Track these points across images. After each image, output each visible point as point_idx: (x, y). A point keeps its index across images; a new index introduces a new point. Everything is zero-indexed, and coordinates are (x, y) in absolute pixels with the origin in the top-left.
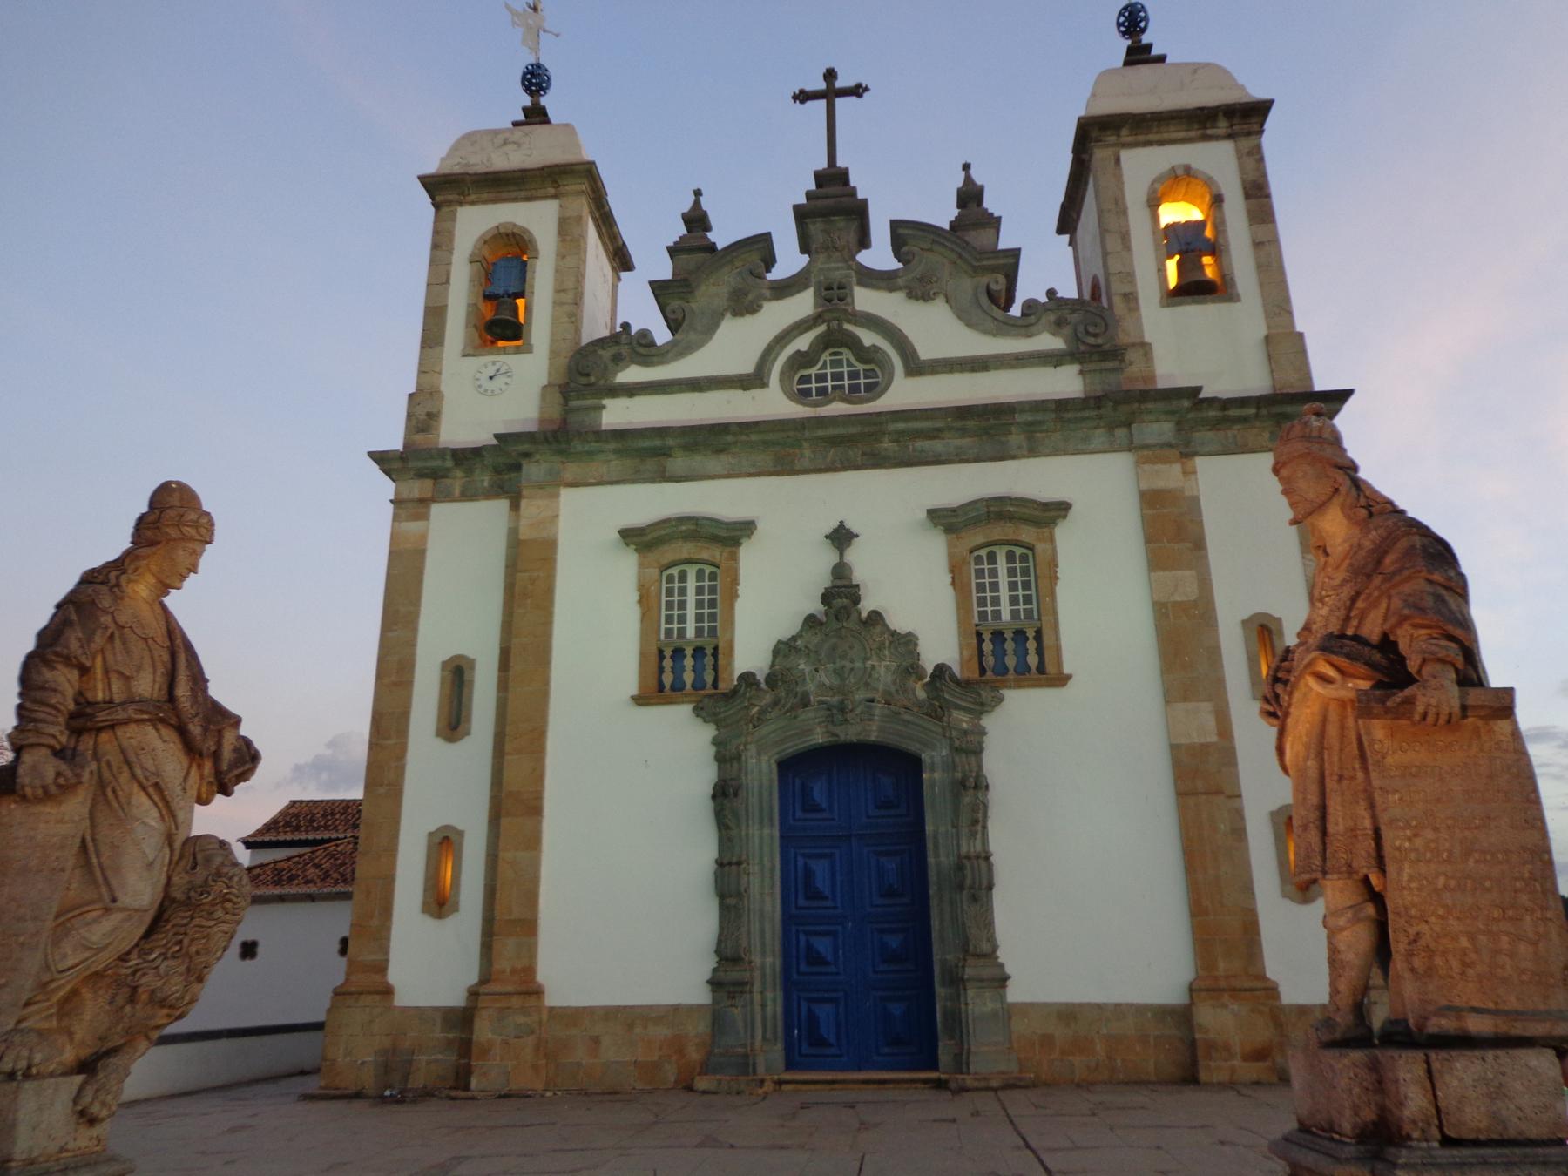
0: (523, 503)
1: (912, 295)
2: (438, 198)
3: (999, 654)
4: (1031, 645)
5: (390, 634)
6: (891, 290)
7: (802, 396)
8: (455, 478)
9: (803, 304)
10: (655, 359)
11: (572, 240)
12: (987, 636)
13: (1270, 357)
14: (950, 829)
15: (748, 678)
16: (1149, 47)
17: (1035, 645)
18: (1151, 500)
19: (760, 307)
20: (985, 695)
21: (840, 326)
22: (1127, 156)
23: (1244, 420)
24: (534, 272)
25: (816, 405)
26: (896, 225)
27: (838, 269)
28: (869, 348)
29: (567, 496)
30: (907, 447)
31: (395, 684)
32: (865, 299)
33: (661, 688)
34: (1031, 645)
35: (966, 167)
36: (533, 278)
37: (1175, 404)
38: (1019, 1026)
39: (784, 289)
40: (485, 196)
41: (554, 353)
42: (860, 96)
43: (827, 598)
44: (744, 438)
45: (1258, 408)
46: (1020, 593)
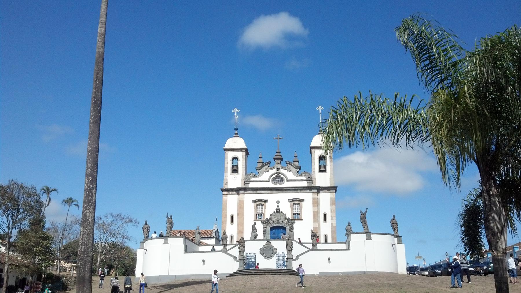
2: (226, 151)
4: (299, 215)
5: (223, 211)
9: (274, 171)
12: (294, 214)
15: (267, 219)
18: (314, 199)
20: (293, 221)
22: (315, 151)
23: (325, 189)
26: (286, 161)
32: (282, 171)
33: (257, 219)
34: (299, 215)
39: (272, 169)
41: (242, 175)
43: (276, 210)
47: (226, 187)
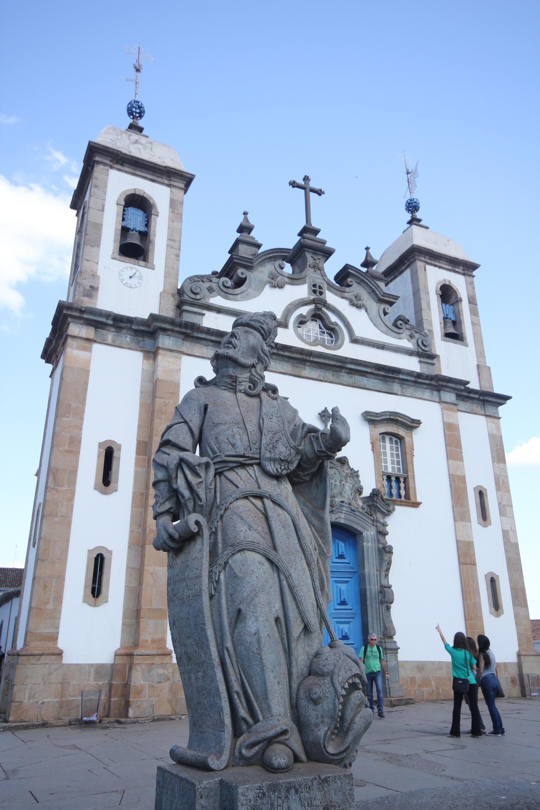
0: (160, 358)
1: (353, 304)
2: (97, 158)
3: (391, 487)
4: (402, 485)
5: (64, 419)
6: (342, 298)
7: (300, 337)
8: (109, 330)
10: (231, 296)
11: (178, 213)
13: (479, 374)
14: (375, 572)
16: (419, 220)
17: (404, 486)
19: (284, 285)
20: (391, 508)
21: (321, 308)
22: (428, 267)
23: (473, 399)
24: (156, 224)
25: (310, 344)
27: (318, 278)
28: (333, 323)
29: (184, 357)
30: (352, 377)
31: (67, 451)
32: (331, 298)
34: (402, 485)
35: (367, 249)
36: (155, 227)
37: (459, 387)
38: (402, 673)
39: (294, 280)
40: (126, 169)
41: (167, 275)
42: (320, 195)
44: (281, 353)
45: (480, 396)
46: (395, 459)
47: (87, 303)
